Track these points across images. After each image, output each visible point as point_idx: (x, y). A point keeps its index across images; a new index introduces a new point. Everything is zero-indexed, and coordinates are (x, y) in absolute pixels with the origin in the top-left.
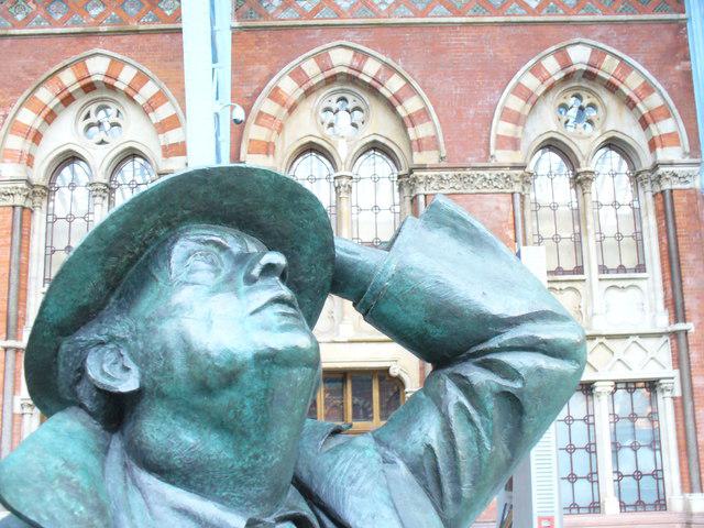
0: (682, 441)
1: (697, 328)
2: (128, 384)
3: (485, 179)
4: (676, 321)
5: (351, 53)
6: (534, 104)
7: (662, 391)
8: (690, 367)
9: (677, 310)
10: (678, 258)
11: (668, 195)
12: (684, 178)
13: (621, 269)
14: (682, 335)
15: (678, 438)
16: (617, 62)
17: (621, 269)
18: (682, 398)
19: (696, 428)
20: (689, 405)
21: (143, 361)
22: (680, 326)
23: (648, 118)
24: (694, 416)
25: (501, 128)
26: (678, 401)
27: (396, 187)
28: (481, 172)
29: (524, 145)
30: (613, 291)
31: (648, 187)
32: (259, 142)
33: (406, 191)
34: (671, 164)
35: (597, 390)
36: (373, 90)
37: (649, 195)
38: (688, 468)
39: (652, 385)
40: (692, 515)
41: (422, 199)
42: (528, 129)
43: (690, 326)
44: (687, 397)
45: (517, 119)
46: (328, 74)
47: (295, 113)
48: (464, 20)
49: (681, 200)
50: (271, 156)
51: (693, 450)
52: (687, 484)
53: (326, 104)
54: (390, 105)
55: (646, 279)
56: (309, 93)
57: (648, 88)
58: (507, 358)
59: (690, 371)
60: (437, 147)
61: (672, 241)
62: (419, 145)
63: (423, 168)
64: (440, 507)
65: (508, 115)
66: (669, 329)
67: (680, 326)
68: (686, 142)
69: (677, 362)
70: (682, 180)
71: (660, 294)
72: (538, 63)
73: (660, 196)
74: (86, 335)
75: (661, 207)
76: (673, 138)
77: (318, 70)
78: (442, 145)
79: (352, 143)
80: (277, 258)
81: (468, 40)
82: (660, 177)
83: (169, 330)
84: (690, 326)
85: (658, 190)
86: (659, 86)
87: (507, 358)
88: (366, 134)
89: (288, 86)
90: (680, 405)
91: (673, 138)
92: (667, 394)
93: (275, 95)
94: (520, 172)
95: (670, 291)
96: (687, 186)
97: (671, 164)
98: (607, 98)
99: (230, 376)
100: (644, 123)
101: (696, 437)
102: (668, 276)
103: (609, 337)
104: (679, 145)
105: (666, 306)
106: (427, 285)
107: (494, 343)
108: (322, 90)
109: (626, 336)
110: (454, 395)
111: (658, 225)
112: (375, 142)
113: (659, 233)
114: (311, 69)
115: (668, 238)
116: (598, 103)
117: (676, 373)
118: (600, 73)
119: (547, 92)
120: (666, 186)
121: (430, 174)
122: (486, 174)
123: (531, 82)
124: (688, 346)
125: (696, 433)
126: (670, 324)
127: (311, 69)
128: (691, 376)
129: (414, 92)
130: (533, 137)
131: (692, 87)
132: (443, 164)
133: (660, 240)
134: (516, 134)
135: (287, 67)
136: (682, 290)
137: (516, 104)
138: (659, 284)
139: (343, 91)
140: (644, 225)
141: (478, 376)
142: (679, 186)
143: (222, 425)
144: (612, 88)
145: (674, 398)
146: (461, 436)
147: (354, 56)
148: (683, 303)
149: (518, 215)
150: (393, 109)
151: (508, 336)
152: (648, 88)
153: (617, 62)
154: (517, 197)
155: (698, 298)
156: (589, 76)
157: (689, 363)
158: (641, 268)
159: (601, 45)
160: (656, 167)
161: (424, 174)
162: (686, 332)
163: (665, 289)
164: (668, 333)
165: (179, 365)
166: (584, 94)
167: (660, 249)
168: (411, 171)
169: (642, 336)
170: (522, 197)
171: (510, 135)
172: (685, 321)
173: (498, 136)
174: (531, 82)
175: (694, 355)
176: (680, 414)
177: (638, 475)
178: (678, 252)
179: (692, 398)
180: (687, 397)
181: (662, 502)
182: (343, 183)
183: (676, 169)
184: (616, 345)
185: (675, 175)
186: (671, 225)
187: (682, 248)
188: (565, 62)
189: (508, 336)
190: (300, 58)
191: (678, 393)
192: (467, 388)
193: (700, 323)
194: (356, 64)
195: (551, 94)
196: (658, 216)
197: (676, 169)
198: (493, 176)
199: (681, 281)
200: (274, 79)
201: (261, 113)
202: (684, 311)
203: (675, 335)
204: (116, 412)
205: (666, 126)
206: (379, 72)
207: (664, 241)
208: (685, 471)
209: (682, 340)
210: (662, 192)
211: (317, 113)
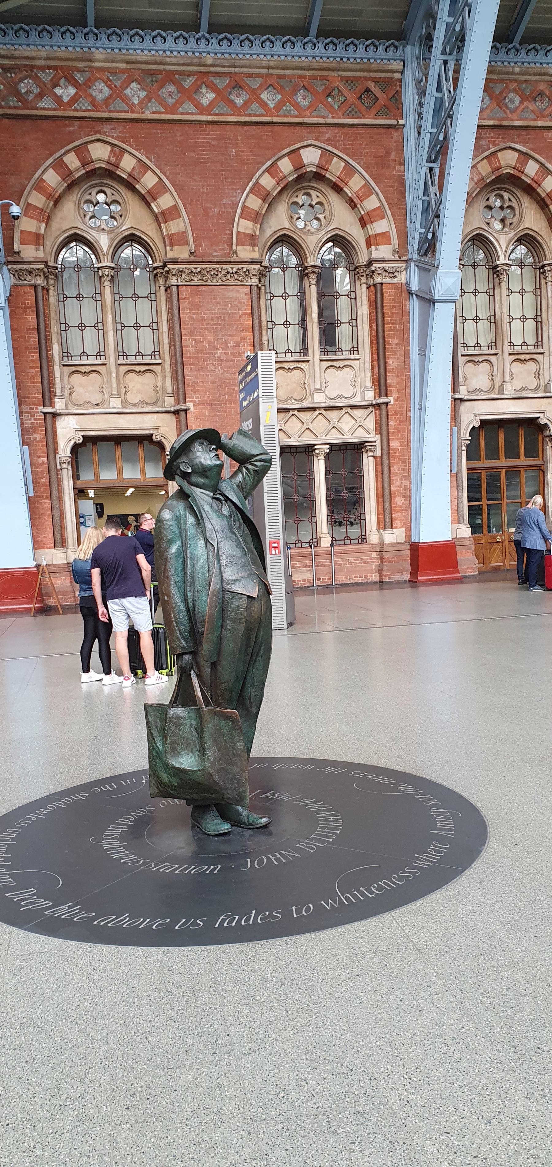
0: (380, 491)
1: (395, 401)
2: (190, 471)
3: (228, 272)
4: (380, 396)
5: (109, 148)
6: (270, 205)
8: (388, 433)
10: (384, 342)
11: (378, 286)
12: (393, 274)
14: (384, 406)
16: (343, 164)
18: (381, 457)
19: (390, 480)
20: (386, 465)
21: (192, 467)
22: (383, 400)
23: (366, 218)
24: (390, 471)
25: (245, 226)
26: (378, 459)
27: (152, 277)
28: (225, 266)
29: (262, 241)
31: (363, 280)
32: (30, 233)
33: (161, 281)
34: (383, 261)
35: (317, 451)
36: (130, 186)
37: (364, 287)
38: (384, 511)
40: (384, 544)
41: (174, 289)
42: (265, 226)
43: (391, 399)
44: (385, 457)
45: (257, 218)
46: (89, 168)
47: (59, 205)
48: (210, 118)
49: (388, 293)
50: (41, 247)
51: (387, 498)
52: (382, 523)
53: (87, 197)
54: (146, 200)
55: (358, 359)
56: (71, 187)
57: (367, 191)
58: (255, 463)
59: (388, 436)
60: (187, 243)
61: (380, 329)
62: (173, 240)
63: (175, 262)
64: (243, 494)
65: (246, 213)
66: (374, 402)
68: (396, 241)
69: (379, 429)
70: (391, 275)
71: (369, 374)
72: (274, 164)
73: (372, 288)
74: (179, 461)
75: (373, 298)
76: (384, 238)
77: (78, 164)
78: (191, 241)
79: (113, 235)
80: (214, 447)
81: (213, 139)
82: (373, 272)
83: (197, 461)
84: (391, 399)
85: (371, 282)
86: (376, 189)
87: (255, 463)
88: (126, 226)
89: (52, 178)
90: (379, 462)
91: (384, 238)
92: (371, 454)
93: (40, 186)
94: (258, 267)
95: (376, 370)
97: (383, 261)
98: (333, 197)
99: (211, 468)
100: (363, 222)
101: (390, 487)
103: (326, 409)
104: (391, 244)
105: (373, 383)
106: (239, 448)
107: (253, 460)
108: (83, 184)
109: (341, 408)
110: (245, 471)
111: (370, 314)
112: (132, 235)
113: (370, 320)
114: (72, 161)
115: (377, 325)
116: (325, 202)
118: (327, 175)
119: (280, 193)
120: (378, 279)
121: (181, 267)
122: (228, 267)
123: (267, 182)
124: (388, 415)
125: (390, 484)
127: (72, 161)
128: (388, 440)
129: (166, 190)
130: (268, 232)
131: (405, 190)
132: (193, 258)
133: (371, 327)
134: (255, 231)
135: (50, 161)
136: (385, 369)
137: (255, 203)
138: (368, 365)
139: (102, 184)
140: (359, 313)
141: (250, 467)
142: (388, 280)
143: (207, 477)
144: (337, 189)
146: (247, 478)
147: (111, 151)
148: (386, 380)
149: (255, 304)
150: (148, 205)
151: (256, 458)
152: (367, 191)
153: (343, 164)
154: (255, 288)
155: (398, 376)
156: (319, 177)
157: (388, 429)
159: (329, 148)
160: (370, 263)
161: (176, 267)
162: (387, 404)
164: (373, 405)
165: (200, 467)
166: (314, 193)
167: (371, 334)
168: (165, 265)
169: (353, 407)
170: (259, 288)
171: (250, 232)
172: (386, 396)
173: (238, 233)
174: (267, 182)
175: (392, 423)
176: (379, 469)
178: (384, 338)
179: (389, 457)
180: (385, 457)
181: (363, 537)
182: (107, 273)
183: (387, 266)
184: (333, 415)
185: (386, 271)
186: (380, 315)
188: (298, 165)
189: (256, 458)
190: (62, 151)
191: (378, 453)
192: (247, 469)
193: (398, 397)
194: (113, 160)
195: (286, 193)
197: (387, 266)
198: (235, 270)
199: (385, 363)
200: (40, 172)
201: (29, 204)
202: (386, 387)
204: (185, 476)
205: (380, 227)
206: (134, 168)
207: (374, 327)
208: (381, 512)
210: (375, 285)
211: (79, 204)
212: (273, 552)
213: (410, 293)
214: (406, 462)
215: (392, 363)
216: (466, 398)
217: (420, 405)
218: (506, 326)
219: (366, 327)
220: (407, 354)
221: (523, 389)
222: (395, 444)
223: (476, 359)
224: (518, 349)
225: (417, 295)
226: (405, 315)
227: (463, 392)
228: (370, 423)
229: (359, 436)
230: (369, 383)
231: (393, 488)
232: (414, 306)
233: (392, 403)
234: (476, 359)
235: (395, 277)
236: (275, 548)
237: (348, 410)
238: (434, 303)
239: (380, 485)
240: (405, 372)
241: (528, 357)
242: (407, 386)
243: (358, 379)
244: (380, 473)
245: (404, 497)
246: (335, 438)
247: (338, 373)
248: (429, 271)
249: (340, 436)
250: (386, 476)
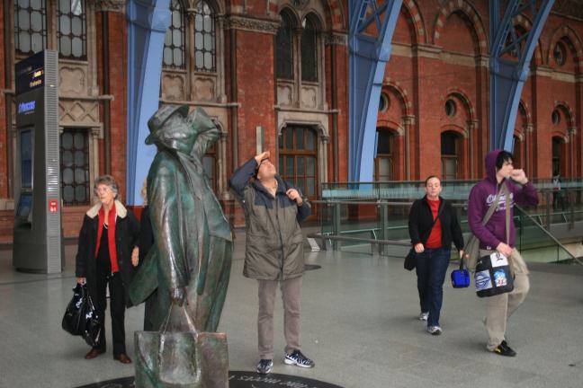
0: (102, 166)
1: (117, 98)
4: (104, 93)
7: (92, 134)
9: (105, 86)
13: (72, 57)
15: (100, 163)
17: (72, 57)
18: (104, 140)
20: (108, 144)
22: (106, 97)
30: (64, 71)
31: (93, 7)
37: (93, 12)
39: (85, 132)
43: (112, 97)
44: (107, 140)
49: (112, 20)
66: (100, 98)
67: (106, 97)
71: (95, 76)
73: (100, 14)
75: (100, 21)
84: (112, 97)
90: (104, 145)
92: (95, 137)
96: (117, 11)
102: (101, 65)
105: (98, 83)
109: (72, 100)
117: (101, 125)
120: (105, 9)
124: (110, 109)
125: (111, 160)
126: (100, 95)
128: (110, 127)
136: (108, 75)
138: (95, 70)
140: (88, 30)
142: (113, 10)
145: (99, 140)
148: (109, 83)
158: (84, 58)
162: (109, 100)
163: (98, 73)
164: (98, 100)
169: (83, 100)
172: (109, 94)
177: (74, 185)
187: (110, 49)
191: (102, 136)
196: (97, 27)
199: (109, 69)
203: (103, 102)
207: (101, 42)
209: (107, 104)
210: (102, 12)
212: (52, 210)
213: (128, 21)
214: (123, 144)
215: (114, 70)
216: (166, 101)
217: (136, 101)
218: (193, 55)
219: (94, 41)
220: (125, 65)
221: (204, 99)
222: (114, 131)
223: (172, 75)
224: (200, 71)
225: (135, 24)
226: (124, 36)
227: (163, 99)
228: (95, 113)
229: (86, 123)
230: (95, 83)
231: (113, 164)
232: (131, 33)
233: (113, 99)
234: (172, 75)
235: (117, 8)
236: (53, 206)
237: (79, 102)
238: (150, 31)
239: (102, 161)
240: (123, 78)
241: (206, 77)
242: (124, 89)
243: (86, 80)
244: (102, 152)
245: (121, 170)
246: (69, 123)
247: (71, 73)
248: (146, 8)
249: (71, 121)
250: (108, 154)
